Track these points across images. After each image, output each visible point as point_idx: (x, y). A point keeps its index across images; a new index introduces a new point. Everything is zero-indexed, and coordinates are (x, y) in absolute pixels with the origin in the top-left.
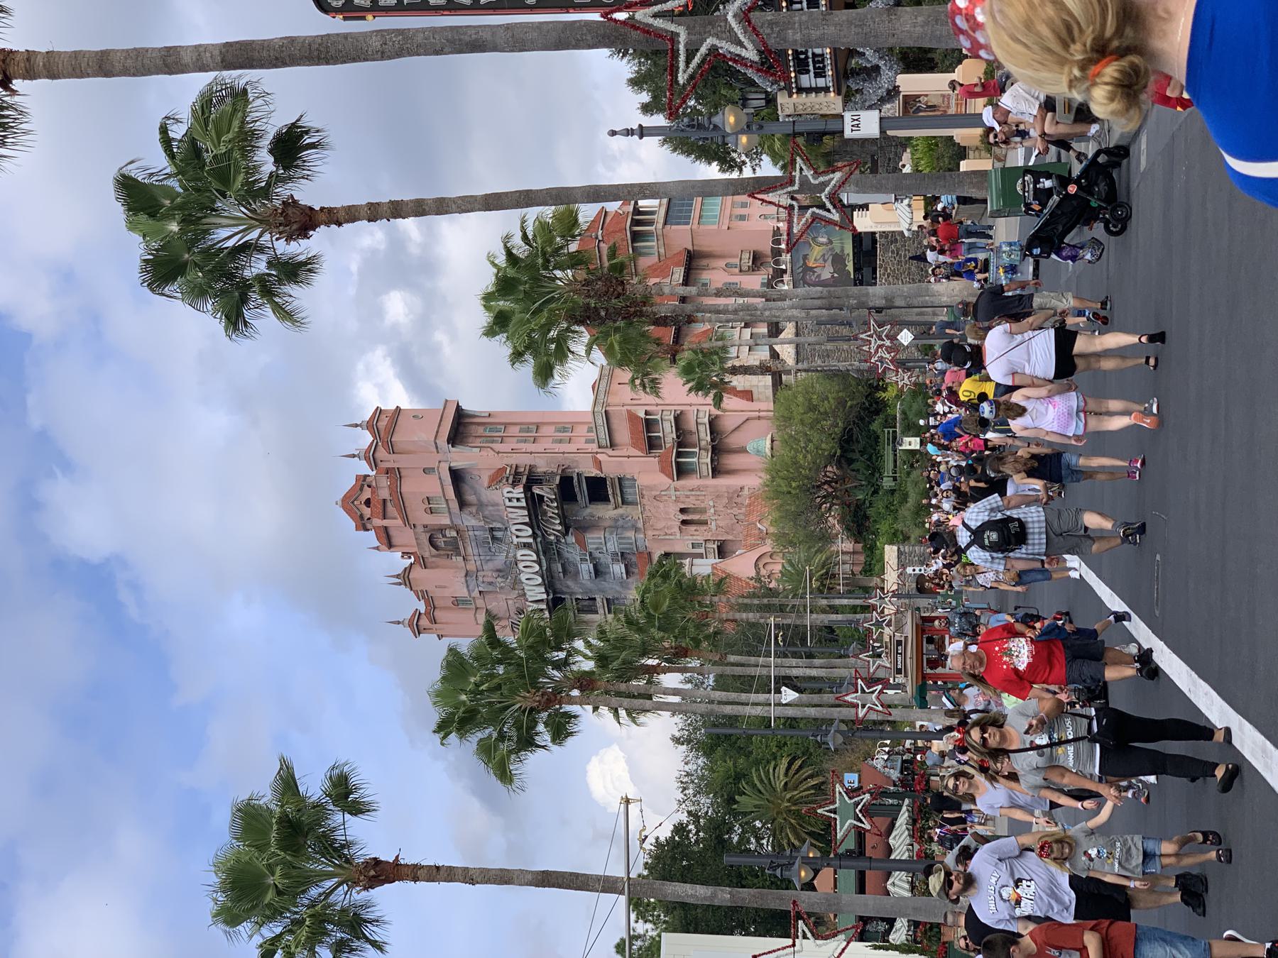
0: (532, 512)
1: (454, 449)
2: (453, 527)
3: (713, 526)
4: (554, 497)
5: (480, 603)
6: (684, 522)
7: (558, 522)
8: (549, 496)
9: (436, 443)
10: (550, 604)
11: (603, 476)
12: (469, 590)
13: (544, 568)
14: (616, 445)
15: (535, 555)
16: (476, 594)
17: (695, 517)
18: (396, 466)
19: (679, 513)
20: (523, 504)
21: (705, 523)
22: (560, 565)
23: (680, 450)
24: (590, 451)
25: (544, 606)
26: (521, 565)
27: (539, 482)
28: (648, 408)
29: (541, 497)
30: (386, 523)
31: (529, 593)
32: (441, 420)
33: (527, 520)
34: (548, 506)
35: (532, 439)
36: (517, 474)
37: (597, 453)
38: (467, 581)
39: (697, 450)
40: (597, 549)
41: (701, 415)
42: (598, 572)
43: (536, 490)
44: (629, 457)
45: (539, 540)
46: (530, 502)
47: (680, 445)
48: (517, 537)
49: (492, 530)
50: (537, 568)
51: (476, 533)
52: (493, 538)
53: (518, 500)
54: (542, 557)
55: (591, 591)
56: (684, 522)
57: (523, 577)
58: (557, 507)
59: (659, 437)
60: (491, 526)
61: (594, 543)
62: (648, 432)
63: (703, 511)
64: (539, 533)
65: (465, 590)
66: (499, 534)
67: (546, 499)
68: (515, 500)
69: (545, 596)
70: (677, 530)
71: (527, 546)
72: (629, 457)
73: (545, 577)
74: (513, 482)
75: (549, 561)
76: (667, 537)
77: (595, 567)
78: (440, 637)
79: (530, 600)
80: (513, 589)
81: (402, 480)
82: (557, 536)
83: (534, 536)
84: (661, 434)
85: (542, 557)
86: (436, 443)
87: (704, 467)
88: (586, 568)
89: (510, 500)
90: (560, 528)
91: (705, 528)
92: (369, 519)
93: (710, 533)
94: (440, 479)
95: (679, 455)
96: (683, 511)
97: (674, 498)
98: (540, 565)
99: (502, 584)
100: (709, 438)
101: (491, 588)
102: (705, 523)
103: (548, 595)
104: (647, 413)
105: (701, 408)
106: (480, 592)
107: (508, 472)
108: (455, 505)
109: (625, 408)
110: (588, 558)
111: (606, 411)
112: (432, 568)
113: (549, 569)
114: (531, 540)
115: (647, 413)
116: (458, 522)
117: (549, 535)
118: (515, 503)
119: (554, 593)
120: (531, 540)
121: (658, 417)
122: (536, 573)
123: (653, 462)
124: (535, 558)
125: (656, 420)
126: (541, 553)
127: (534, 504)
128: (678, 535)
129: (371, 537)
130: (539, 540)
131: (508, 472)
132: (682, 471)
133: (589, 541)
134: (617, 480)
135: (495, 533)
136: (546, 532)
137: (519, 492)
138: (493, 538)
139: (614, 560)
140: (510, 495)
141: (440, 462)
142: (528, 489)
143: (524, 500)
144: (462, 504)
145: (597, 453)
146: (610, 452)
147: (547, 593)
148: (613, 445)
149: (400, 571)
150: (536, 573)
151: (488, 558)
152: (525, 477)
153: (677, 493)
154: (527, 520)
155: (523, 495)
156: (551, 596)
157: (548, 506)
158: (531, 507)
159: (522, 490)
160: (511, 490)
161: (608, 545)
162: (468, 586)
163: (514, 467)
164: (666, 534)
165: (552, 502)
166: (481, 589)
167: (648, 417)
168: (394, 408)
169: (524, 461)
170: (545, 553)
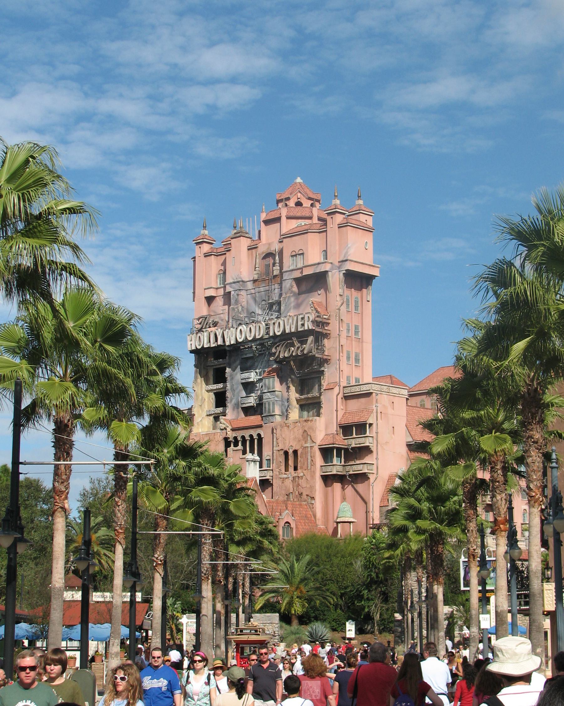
1: (341, 275)
4: (305, 352)
6: (286, 453)
7: (286, 355)
9: (346, 260)
10: (222, 348)
15: (259, 337)
16: (228, 289)
17: (291, 462)
18: (328, 229)
19: (294, 449)
20: (300, 329)
21: (287, 469)
24: (341, 380)
25: (220, 342)
26: (252, 326)
27: (317, 340)
28: (374, 426)
29: (305, 342)
30: (284, 219)
32: (362, 263)
33: (287, 331)
36: (324, 324)
37: (340, 386)
38: (238, 282)
39: (343, 463)
40: (265, 385)
41: (370, 467)
42: (249, 387)
43: (311, 339)
44: (337, 411)
47: (346, 450)
50: (250, 339)
53: (303, 325)
55: (232, 379)
56: (286, 453)
59: (352, 435)
61: (269, 382)
63: (296, 469)
64: (277, 340)
65: (231, 281)
68: (302, 323)
72: (337, 411)
79: (225, 332)
81: (317, 234)
82: (275, 353)
83: (275, 336)
84: (354, 436)
86: (346, 260)
87: (329, 469)
89: (303, 318)
92: (286, 205)
93: (278, 473)
94: (319, 264)
95: (339, 450)
96: (295, 452)
97: (305, 445)
99: (236, 309)
100: (351, 473)
102: (287, 469)
103: (228, 346)
104: (371, 425)
105: (374, 467)
108: (297, 274)
109: (375, 408)
111: (372, 393)
112: (248, 254)
114: (271, 334)
115: (371, 425)
117: (276, 348)
118: (300, 323)
120: (271, 334)
121: (368, 434)
123: (334, 428)
124: (258, 337)
127: (302, 336)
131: (325, 317)
132: (326, 453)
136: (278, 346)
137: (309, 326)
140: (306, 318)
141: (332, 263)
142: (310, 332)
143: (302, 329)
144: (298, 281)
146: (341, 395)
147: (231, 345)
151: (257, 299)
153: (309, 449)
154: (287, 331)
155: (306, 328)
156: (227, 348)
159: (310, 328)
161: (268, 394)
162: (234, 283)
166: (233, 293)
167: (368, 425)
169: (333, 327)
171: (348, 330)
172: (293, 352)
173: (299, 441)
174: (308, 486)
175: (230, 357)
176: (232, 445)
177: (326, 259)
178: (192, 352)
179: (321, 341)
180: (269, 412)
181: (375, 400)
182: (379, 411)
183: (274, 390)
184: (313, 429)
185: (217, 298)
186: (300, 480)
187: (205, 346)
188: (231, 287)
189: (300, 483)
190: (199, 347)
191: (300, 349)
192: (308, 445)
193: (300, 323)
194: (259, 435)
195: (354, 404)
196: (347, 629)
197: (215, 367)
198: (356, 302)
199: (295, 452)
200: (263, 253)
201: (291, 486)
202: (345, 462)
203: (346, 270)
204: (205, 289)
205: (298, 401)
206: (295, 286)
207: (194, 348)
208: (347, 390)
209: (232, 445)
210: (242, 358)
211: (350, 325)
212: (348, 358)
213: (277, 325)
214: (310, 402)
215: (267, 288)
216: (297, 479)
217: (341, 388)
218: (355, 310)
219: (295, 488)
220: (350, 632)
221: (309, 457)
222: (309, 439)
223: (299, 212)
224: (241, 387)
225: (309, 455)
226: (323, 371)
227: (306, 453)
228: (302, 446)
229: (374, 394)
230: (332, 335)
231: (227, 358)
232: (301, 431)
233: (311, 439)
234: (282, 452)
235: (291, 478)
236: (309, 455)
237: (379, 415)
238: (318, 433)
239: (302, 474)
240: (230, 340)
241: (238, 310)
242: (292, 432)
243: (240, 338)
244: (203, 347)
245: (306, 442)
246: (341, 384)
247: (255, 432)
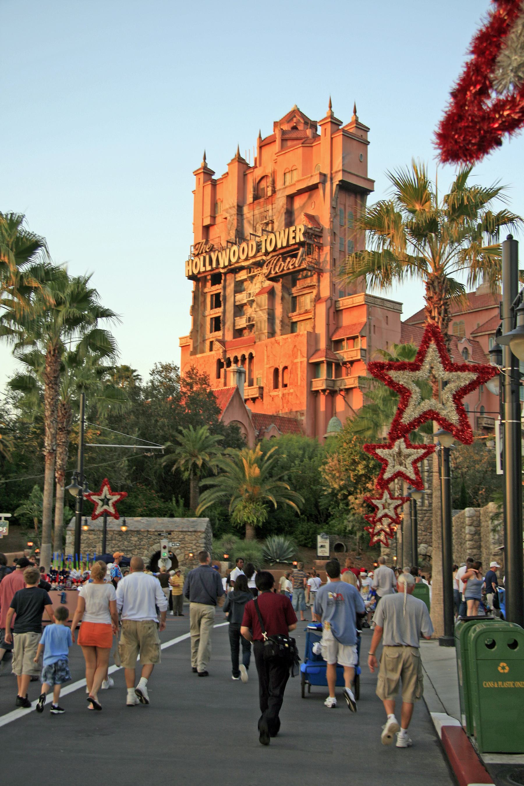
0: (285, 250)
2: (274, 192)
3: (274, 393)
4: (297, 266)
5: (219, 220)
8: (297, 262)
10: (217, 271)
12: (227, 209)
13: (243, 264)
20: (292, 242)
21: (276, 387)
22: (245, 277)
23: (334, 364)
26: (244, 245)
29: (295, 256)
31: (224, 252)
33: (279, 246)
34: (289, 262)
35: (343, 250)
38: (234, 207)
45: (264, 258)
46: (292, 248)
48: (266, 240)
49: (273, 222)
50: (243, 257)
51: (270, 211)
52: (267, 224)
53: (294, 238)
54: (251, 261)
56: (276, 371)
57: (235, 248)
58: (289, 269)
60: (275, 221)
62: (348, 339)
66: (269, 228)
67: (294, 259)
69: (222, 265)
70: (272, 364)
71: (258, 250)
73: (236, 265)
74: (308, 233)
75: (249, 268)
76: (266, 357)
77: (245, 304)
78: (194, 192)
80: (228, 242)
83: (267, 253)
88: (242, 298)
89: (294, 231)
90: (273, 272)
91: (272, 388)
97: (295, 361)
98: (247, 259)
101: (229, 226)
103: (223, 268)
107: (317, 230)
110: (251, 298)
113: (242, 268)
114: (263, 251)
117: (267, 266)
118: (292, 235)
119: (225, 274)
122: (239, 258)
124: (251, 255)
128: (268, 366)
129: (268, 132)
130: (264, 258)
131: (317, 230)
135: (270, 225)
136: (269, 262)
137: (300, 237)
138: (267, 224)
139: (249, 320)
140: (298, 230)
142: (301, 244)
143: (294, 242)
144: (291, 198)
145: (331, 300)
147: (225, 267)
149: (243, 156)
150: (239, 258)
153: (299, 364)
154: (279, 246)
155: (298, 241)
156: (222, 271)
157: (289, 262)
158: (288, 249)
159: (302, 239)
160: (302, 231)
162: (230, 208)
163: (320, 234)
164: (268, 357)
165: (292, 265)
166: (229, 218)
168: (369, 140)
170: (254, 264)
173: (289, 357)
174: (298, 402)
176: (225, 366)
178: (190, 278)
180: (261, 330)
182: (372, 324)
185: (215, 226)
186: (290, 397)
187: (201, 271)
188: (227, 213)
189: (290, 400)
190: (196, 272)
191: (291, 263)
193: (292, 235)
194: (251, 355)
196: (319, 545)
199: (285, 368)
201: (281, 403)
202: (336, 377)
203: (340, 181)
207: (191, 274)
209: (225, 366)
215: (262, 210)
216: (287, 396)
219: (285, 405)
220: (323, 549)
221: (299, 373)
223: (294, 135)
225: (299, 370)
227: (296, 368)
228: (292, 362)
231: (222, 281)
232: (291, 347)
233: (301, 354)
234: (272, 370)
235: (281, 395)
236: (299, 370)
237: (372, 328)
239: (292, 391)
240: (224, 261)
244: (199, 273)
245: (296, 358)
247: (247, 351)
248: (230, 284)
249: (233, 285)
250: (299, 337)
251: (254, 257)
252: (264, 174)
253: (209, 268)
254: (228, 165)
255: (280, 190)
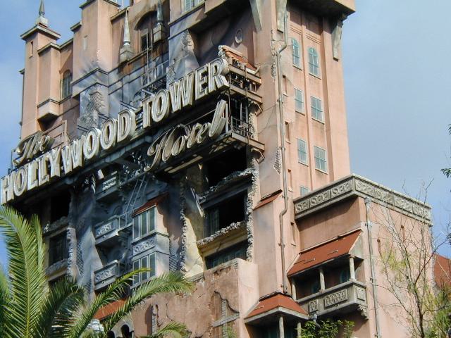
10: (60, 184)
11: (249, 210)
12: (81, 80)
14: (300, 229)
16: (76, 90)
25: (55, 172)
28: (366, 264)
33: (175, 109)
34: (197, 131)
43: (222, 106)
53: (205, 85)
54: (123, 152)
65: (81, 76)
85: (123, 152)
89: (205, 74)
98: (114, 150)
103: (71, 175)
104: (358, 262)
106: (78, 97)
114: (146, 124)
115: (358, 262)
116: (174, 31)
122: (100, 147)
123: (279, 282)
125: (347, 275)
126: (129, 149)
133: (148, 215)
134: (243, 238)
142: (218, 94)
144: (198, 32)
146: (289, 218)
148: (302, 222)
152: (242, 92)
155: (211, 88)
156: (68, 182)
161: (143, 244)
162: (86, 77)
170: (128, 158)
171: (299, 102)
172: (186, 142)
175: (77, 203)
177: (256, 68)
179: (244, 115)
181: (362, 212)
182: (374, 237)
183: (153, 232)
184: (233, 286)
188: (80, 86)
192: (223, 320)
195: (319, 234)
197: (52, 236)
198: (312, 56)
200: (136, 18)
204: (38, 107)
205: (201, 249)
206: (192, 43)
207: (10, 197)
208: (302, 207)
210: (99, 201)
211: (303, 94)
212: (302, 152)
213: (155, 105)
214: (226, 246)
217: (290, 203)
218: (311, 70)
222: (224, 307)
224: (95, 254)
226: (251, 175)
229: (361, 201)
230: (265, 106)
232: (207, 296)
233: (229, 306)
238: (242, 291)
241: (92, 118)
242: (189, 303)
243: (89, 153)
246: (289, 195)
248: (85, 208)
249: (90, 208)
250: (224, 273)
251: (128, 141)
252: (147, 11)
253: (41, 182)
254: (83, 7)
255: (176, 22)
